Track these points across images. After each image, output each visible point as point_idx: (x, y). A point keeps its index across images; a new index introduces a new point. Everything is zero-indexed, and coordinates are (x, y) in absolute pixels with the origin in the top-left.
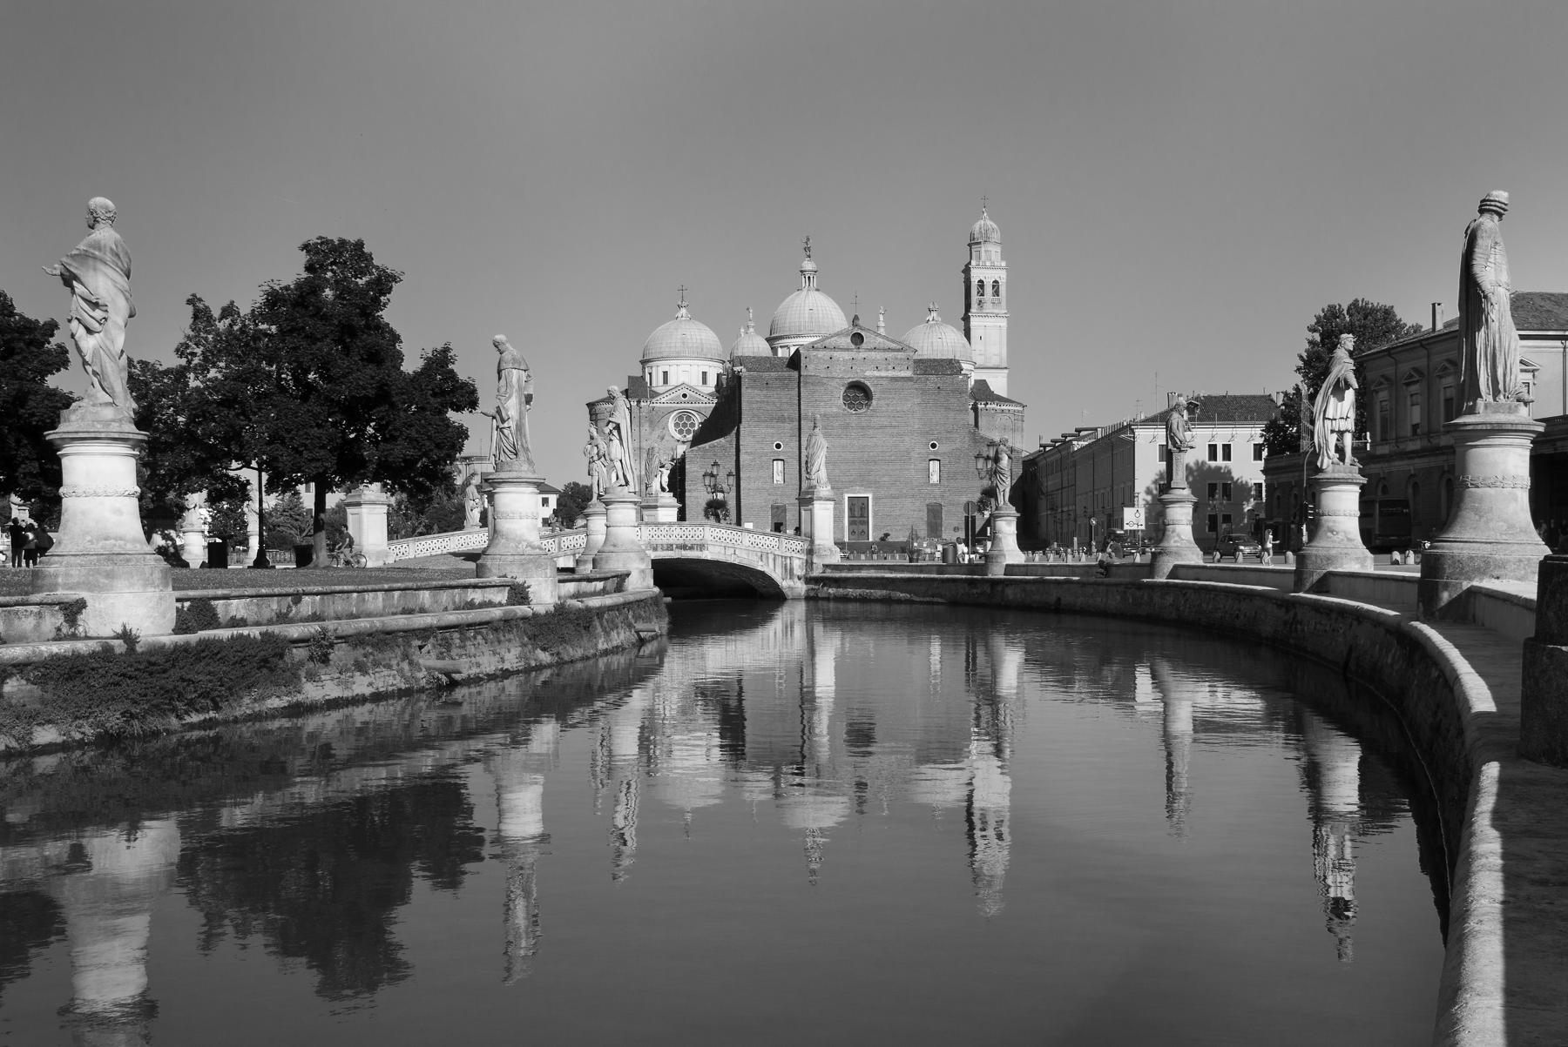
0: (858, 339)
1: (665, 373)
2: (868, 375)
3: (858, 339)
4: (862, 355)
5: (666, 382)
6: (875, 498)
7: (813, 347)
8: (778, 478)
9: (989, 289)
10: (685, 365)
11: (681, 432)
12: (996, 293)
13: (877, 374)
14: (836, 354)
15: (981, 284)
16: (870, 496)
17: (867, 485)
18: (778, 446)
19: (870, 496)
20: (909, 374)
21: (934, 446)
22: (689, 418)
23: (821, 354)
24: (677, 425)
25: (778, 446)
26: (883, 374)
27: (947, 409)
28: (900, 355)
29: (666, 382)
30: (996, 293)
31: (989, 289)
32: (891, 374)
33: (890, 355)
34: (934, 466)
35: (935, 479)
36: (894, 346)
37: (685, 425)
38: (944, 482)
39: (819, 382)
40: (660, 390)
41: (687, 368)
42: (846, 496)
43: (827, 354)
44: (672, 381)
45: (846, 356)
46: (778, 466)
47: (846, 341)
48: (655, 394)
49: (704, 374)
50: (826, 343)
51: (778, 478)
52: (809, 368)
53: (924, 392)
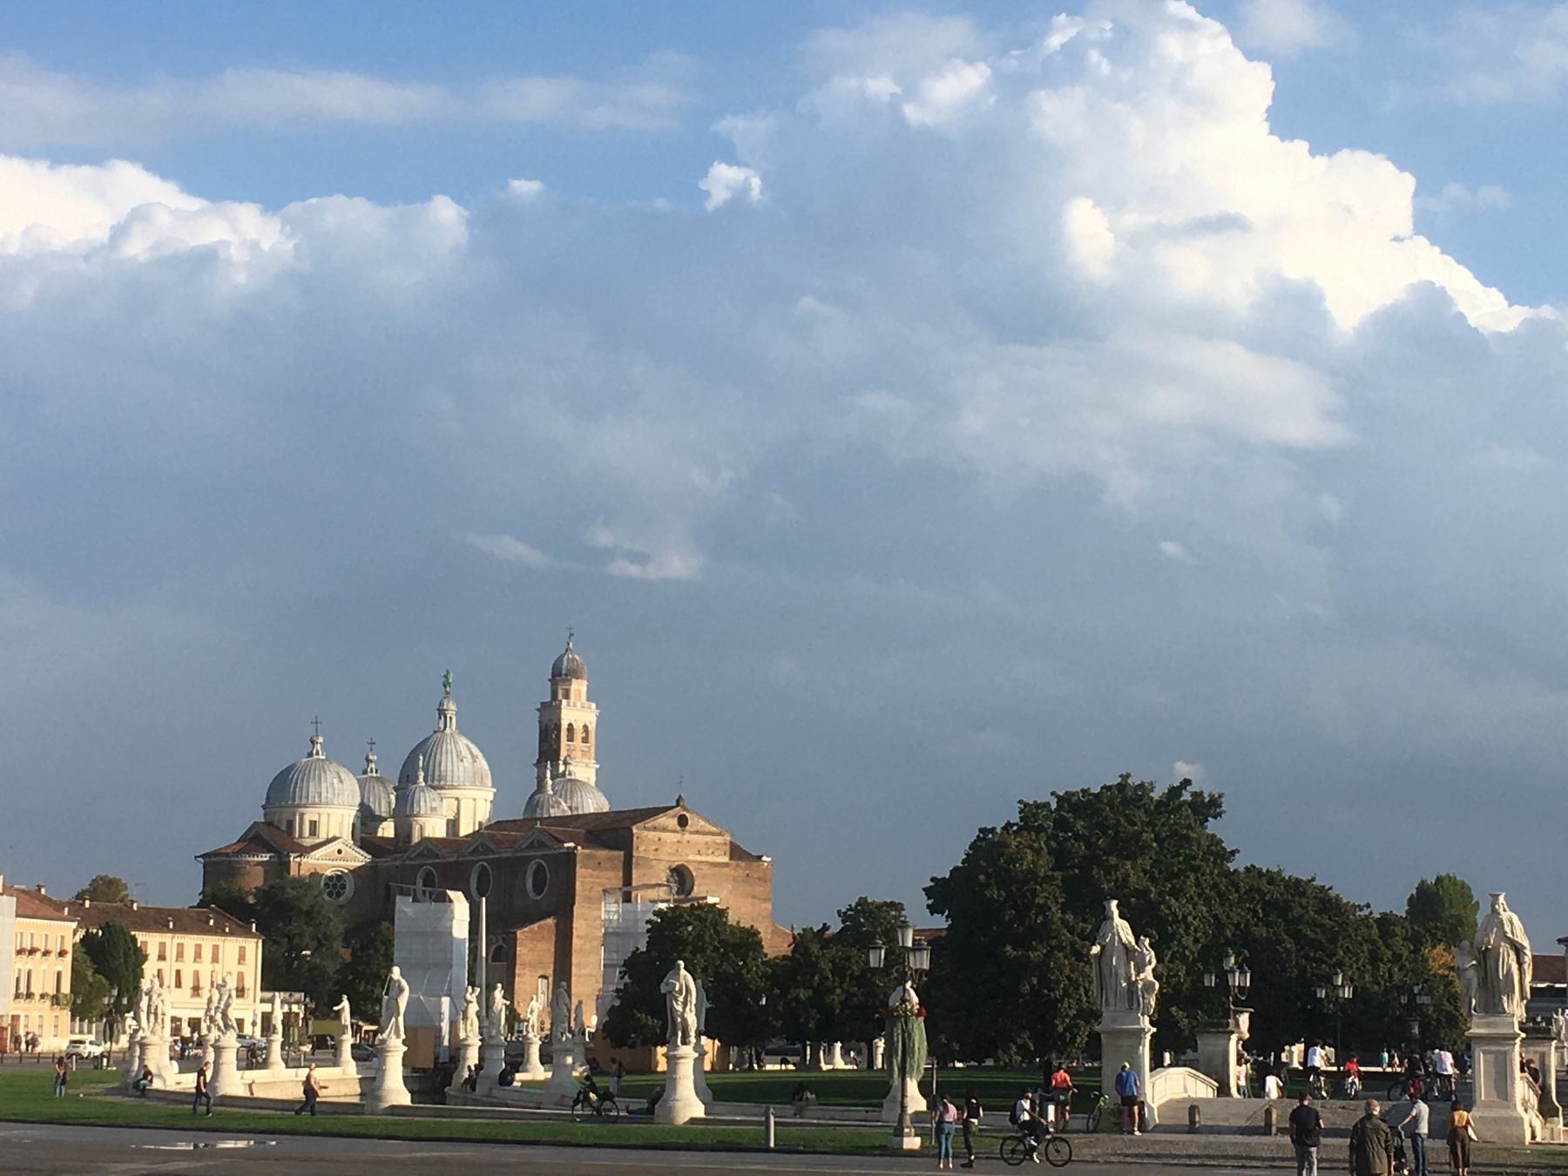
0: (683, 821)
2: (690, 858)
3: (683, 821)
4: (687, 837)
9: (579, 735)
12: (585, 740)
13: (699, 858)
14: (664, 835)
20: (726, 859)
23: (651, 834)
26: (703, 858)
27: (754, 897)
28: (719, 839)
29: (313, 832)
30: (585, 740)
31: (579, 735)
32: (710, 859)
33: (709, 838)
37: (335, 886)
40: (308, 842)
52: (640, 850)
53: (735, 880)
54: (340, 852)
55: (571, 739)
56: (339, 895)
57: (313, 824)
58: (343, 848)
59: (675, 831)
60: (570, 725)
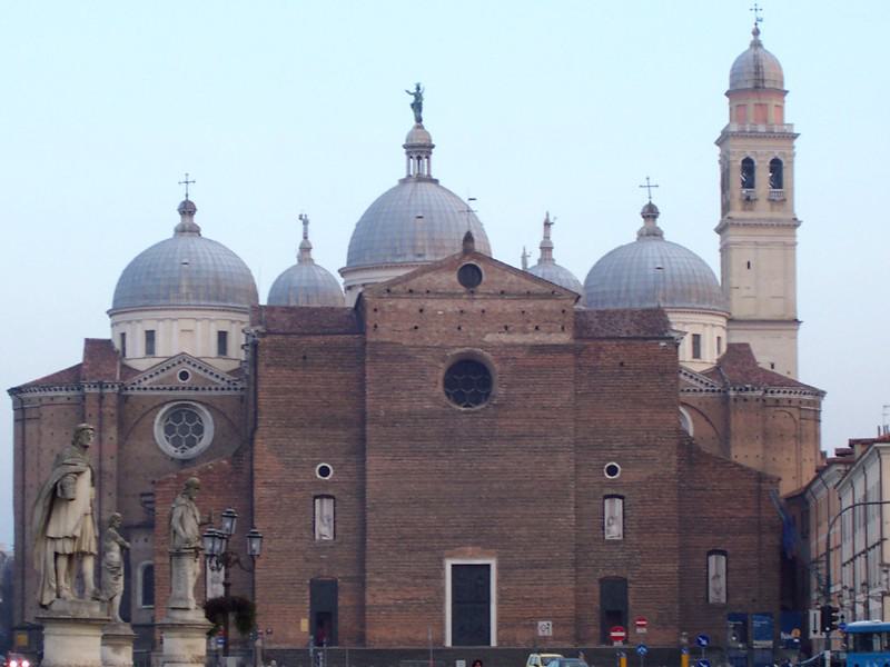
1: (150, 336)
4: (478, 305)
5: (150, 350)
6: (499, 568)
7: (389, 290)
8: (324, 530)
9: (763, 175)
10: (187, 319)
11: (176, 443)
13: (505, 338)
14: (430, 304)
15: (748, 166)
16: (493, 563)
17: (486, 544)
18: (324, 471)
19: (493, 563)
20: (564, 338)
21: (612, 471)
22: (193, 416)
23: (402, 304)
24: (169, 430)
25: (324, 471)
26: (518, 339)
28: (548, 305)
29: (150, 350)
31: (763, 175)
33: (530, 305)
34: (614, 509)
35: (614, 531)
36: (536, 288)
37: (184, 430)
38: (633, 538)
39: (397, 354)
41: (189, 325)
42: (448, 564)
43: (418, 304)
44: (164, 348)
45: (450, 306)
46: (324, 509)
47: (450, 279)
48: (128, 371)
49: (222, 336)
50: (413, 284)
51: (324, 530)
52: (384, 331)
54: (184, 375)
55: (749, 183)
56: (192, 443)
57: (150, 336)
58: (188, 368)
59: (452, 295)
60: (748, 166)
